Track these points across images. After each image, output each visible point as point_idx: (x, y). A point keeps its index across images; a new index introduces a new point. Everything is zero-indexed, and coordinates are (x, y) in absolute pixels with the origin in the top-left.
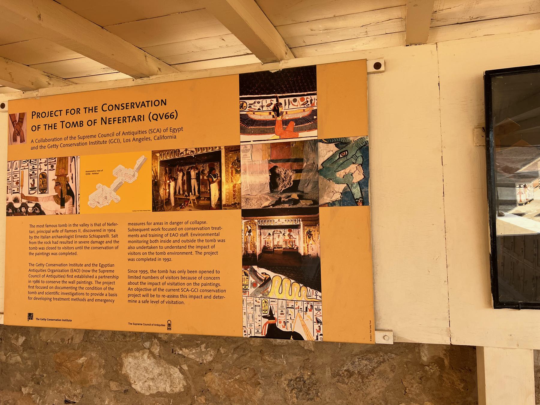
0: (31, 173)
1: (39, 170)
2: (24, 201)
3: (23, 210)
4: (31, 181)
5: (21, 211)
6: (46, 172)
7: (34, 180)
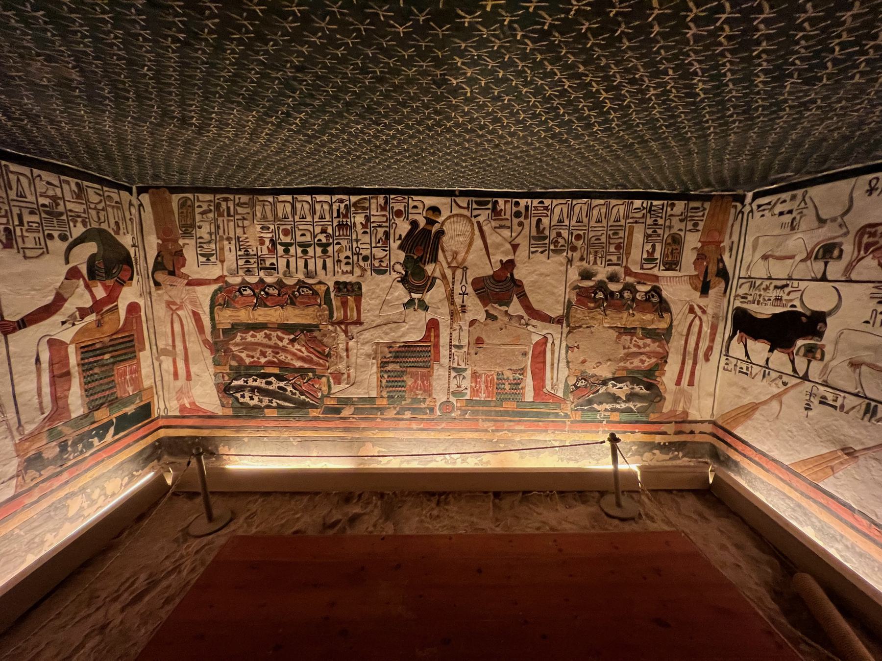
0: (649, 232)
1: (667, 230)
2: (630, 280)
3: (627, 294)
4: (648, 247)
5: (622, 296)
6: (682, 234)
7: (654, 247)
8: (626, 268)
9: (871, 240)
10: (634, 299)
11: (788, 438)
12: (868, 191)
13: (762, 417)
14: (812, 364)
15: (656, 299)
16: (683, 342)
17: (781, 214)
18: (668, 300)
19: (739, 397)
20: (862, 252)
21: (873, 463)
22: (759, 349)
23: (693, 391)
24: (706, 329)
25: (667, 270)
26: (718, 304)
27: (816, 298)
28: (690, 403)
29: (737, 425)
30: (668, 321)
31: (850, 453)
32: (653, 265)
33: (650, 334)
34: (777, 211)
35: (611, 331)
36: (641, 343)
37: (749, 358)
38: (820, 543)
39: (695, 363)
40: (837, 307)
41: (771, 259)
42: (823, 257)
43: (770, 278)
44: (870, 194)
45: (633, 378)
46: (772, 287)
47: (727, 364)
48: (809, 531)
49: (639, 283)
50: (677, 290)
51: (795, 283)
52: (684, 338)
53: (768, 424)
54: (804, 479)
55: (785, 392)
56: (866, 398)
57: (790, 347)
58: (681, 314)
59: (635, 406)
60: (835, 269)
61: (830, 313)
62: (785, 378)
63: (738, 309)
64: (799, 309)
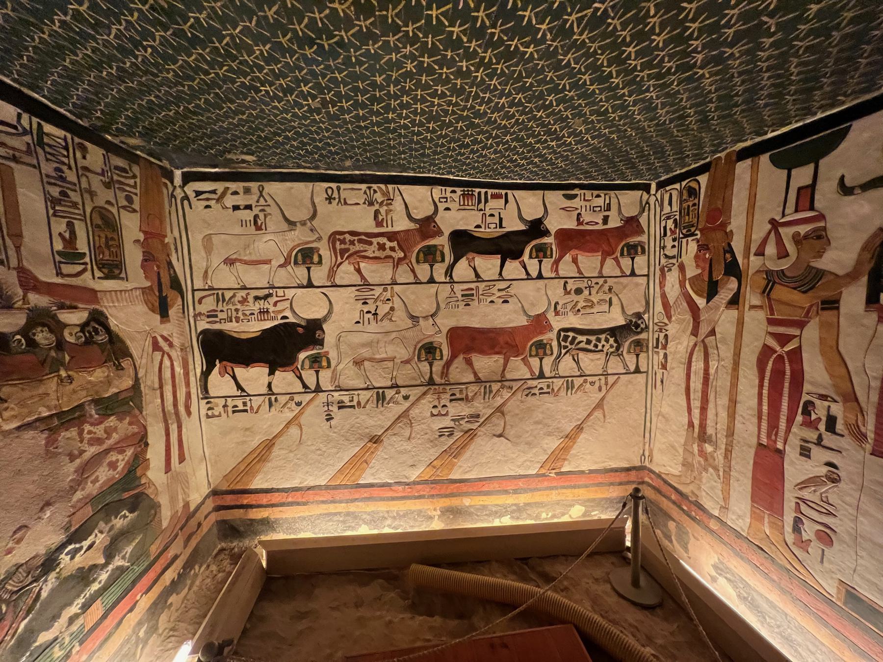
0: (55, 192)
3: (42, 337)
4: (60, 226)
5: (32, 343)
6: (114, 210)
7: (70, 225)
8: (22, 271)
9: (343, 246)
10: (60, 345)
11: (319, 458)
12: (326, 199)
13: (284, 452)
14: (320, 373)
15: (102, 338)
16: (159, 401)
17: (236, 208)
18: (121, 334)
19: (244, 442)
20: (339, 258)
21: (394, 438)
22: (254, 376)
23: (187, 467)
24: (179, 370)
25: (106, 277)
26: (182, 330)
27: (308, 307)
28: (188, 488)
29: (254, 477)
30: (131, 371)
31: (376, 440)
32: (80, 268)
33: (109, 406)
34: (230, 201)
35: (29, 434)
36: (99, 431)
37: (243, 390)
38: (375, 532)
39: (180, 427)
40: (330, 312)
41: (238, 264)
42: (304, 263)
43: (244, 288)
44: (330, 203)
45: (106, 506)
46: (251, 299)
47: (209, 409)
48: (364, 530)
49: (62, 307)
50: (129, 317)
51: (280, 292)
52: (158, 392)
53: (292, 455)
54: (346, 486)
55: (300, 413)
56: (375, 388)
57: (293, 364)
58: (145, 355)
59: (124, 558)
60: (319, 275)
61: (325, 319)
62: (297, 398)
63: (205, 332)
64: (292, 320)
